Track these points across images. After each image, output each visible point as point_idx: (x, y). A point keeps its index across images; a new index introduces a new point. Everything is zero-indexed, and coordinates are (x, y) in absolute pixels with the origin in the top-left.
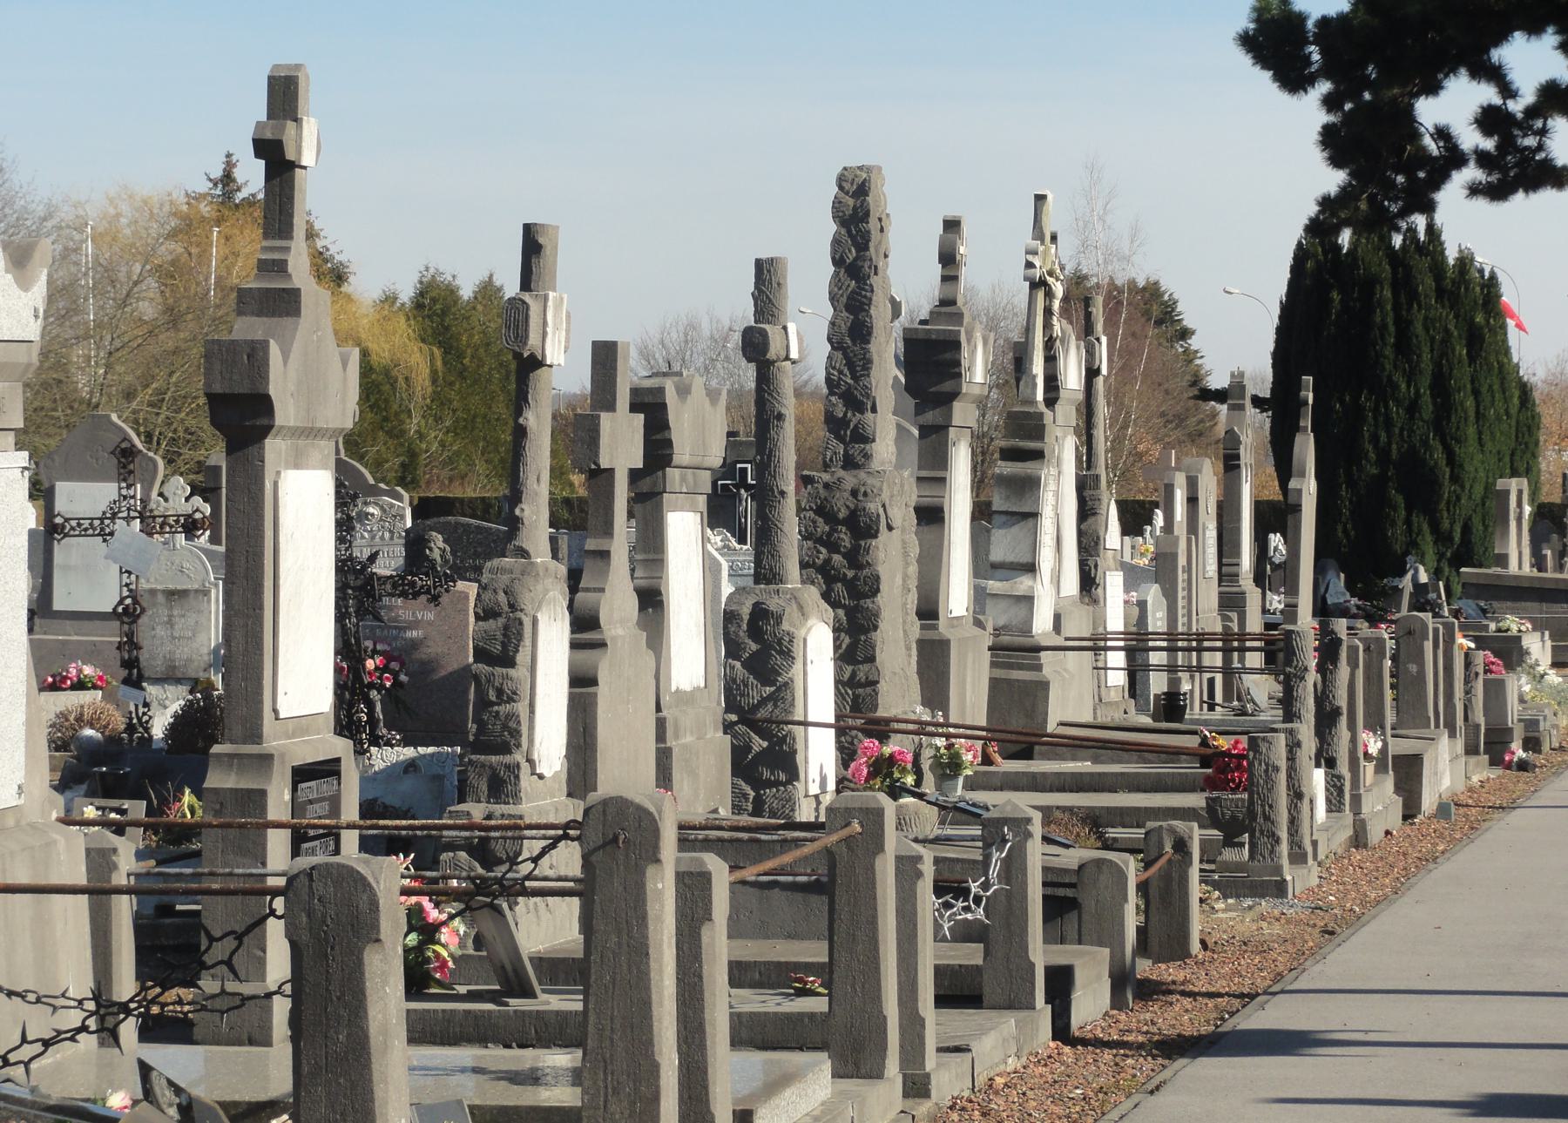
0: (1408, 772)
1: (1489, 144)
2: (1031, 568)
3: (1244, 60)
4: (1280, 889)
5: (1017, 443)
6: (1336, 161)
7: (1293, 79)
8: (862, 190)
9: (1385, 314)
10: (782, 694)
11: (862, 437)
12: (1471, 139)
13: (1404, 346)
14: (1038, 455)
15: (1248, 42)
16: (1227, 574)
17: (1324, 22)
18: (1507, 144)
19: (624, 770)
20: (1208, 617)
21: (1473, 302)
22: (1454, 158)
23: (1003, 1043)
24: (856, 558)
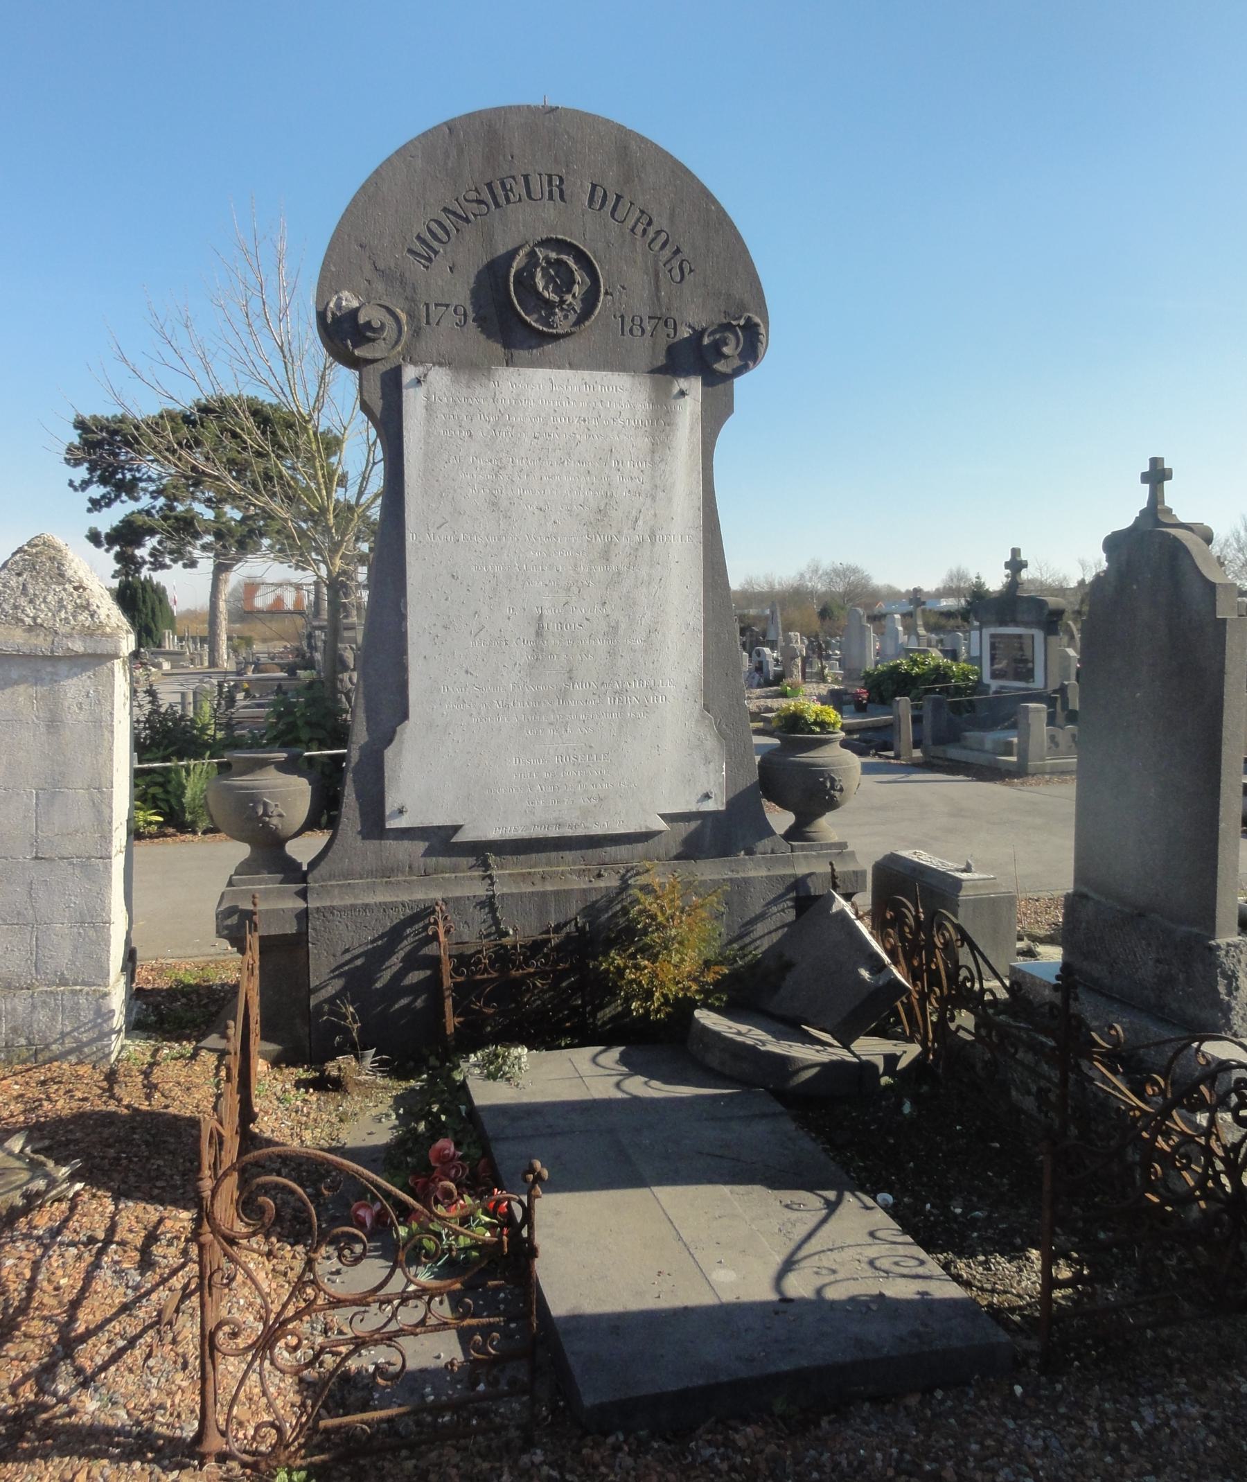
6: (118, 562)
9: (140, 595)
12: (148, 558)
13: (144, 602)
15: (87, 537)
18: (156, 560)
21: (158, 593)
22: (145, 562)
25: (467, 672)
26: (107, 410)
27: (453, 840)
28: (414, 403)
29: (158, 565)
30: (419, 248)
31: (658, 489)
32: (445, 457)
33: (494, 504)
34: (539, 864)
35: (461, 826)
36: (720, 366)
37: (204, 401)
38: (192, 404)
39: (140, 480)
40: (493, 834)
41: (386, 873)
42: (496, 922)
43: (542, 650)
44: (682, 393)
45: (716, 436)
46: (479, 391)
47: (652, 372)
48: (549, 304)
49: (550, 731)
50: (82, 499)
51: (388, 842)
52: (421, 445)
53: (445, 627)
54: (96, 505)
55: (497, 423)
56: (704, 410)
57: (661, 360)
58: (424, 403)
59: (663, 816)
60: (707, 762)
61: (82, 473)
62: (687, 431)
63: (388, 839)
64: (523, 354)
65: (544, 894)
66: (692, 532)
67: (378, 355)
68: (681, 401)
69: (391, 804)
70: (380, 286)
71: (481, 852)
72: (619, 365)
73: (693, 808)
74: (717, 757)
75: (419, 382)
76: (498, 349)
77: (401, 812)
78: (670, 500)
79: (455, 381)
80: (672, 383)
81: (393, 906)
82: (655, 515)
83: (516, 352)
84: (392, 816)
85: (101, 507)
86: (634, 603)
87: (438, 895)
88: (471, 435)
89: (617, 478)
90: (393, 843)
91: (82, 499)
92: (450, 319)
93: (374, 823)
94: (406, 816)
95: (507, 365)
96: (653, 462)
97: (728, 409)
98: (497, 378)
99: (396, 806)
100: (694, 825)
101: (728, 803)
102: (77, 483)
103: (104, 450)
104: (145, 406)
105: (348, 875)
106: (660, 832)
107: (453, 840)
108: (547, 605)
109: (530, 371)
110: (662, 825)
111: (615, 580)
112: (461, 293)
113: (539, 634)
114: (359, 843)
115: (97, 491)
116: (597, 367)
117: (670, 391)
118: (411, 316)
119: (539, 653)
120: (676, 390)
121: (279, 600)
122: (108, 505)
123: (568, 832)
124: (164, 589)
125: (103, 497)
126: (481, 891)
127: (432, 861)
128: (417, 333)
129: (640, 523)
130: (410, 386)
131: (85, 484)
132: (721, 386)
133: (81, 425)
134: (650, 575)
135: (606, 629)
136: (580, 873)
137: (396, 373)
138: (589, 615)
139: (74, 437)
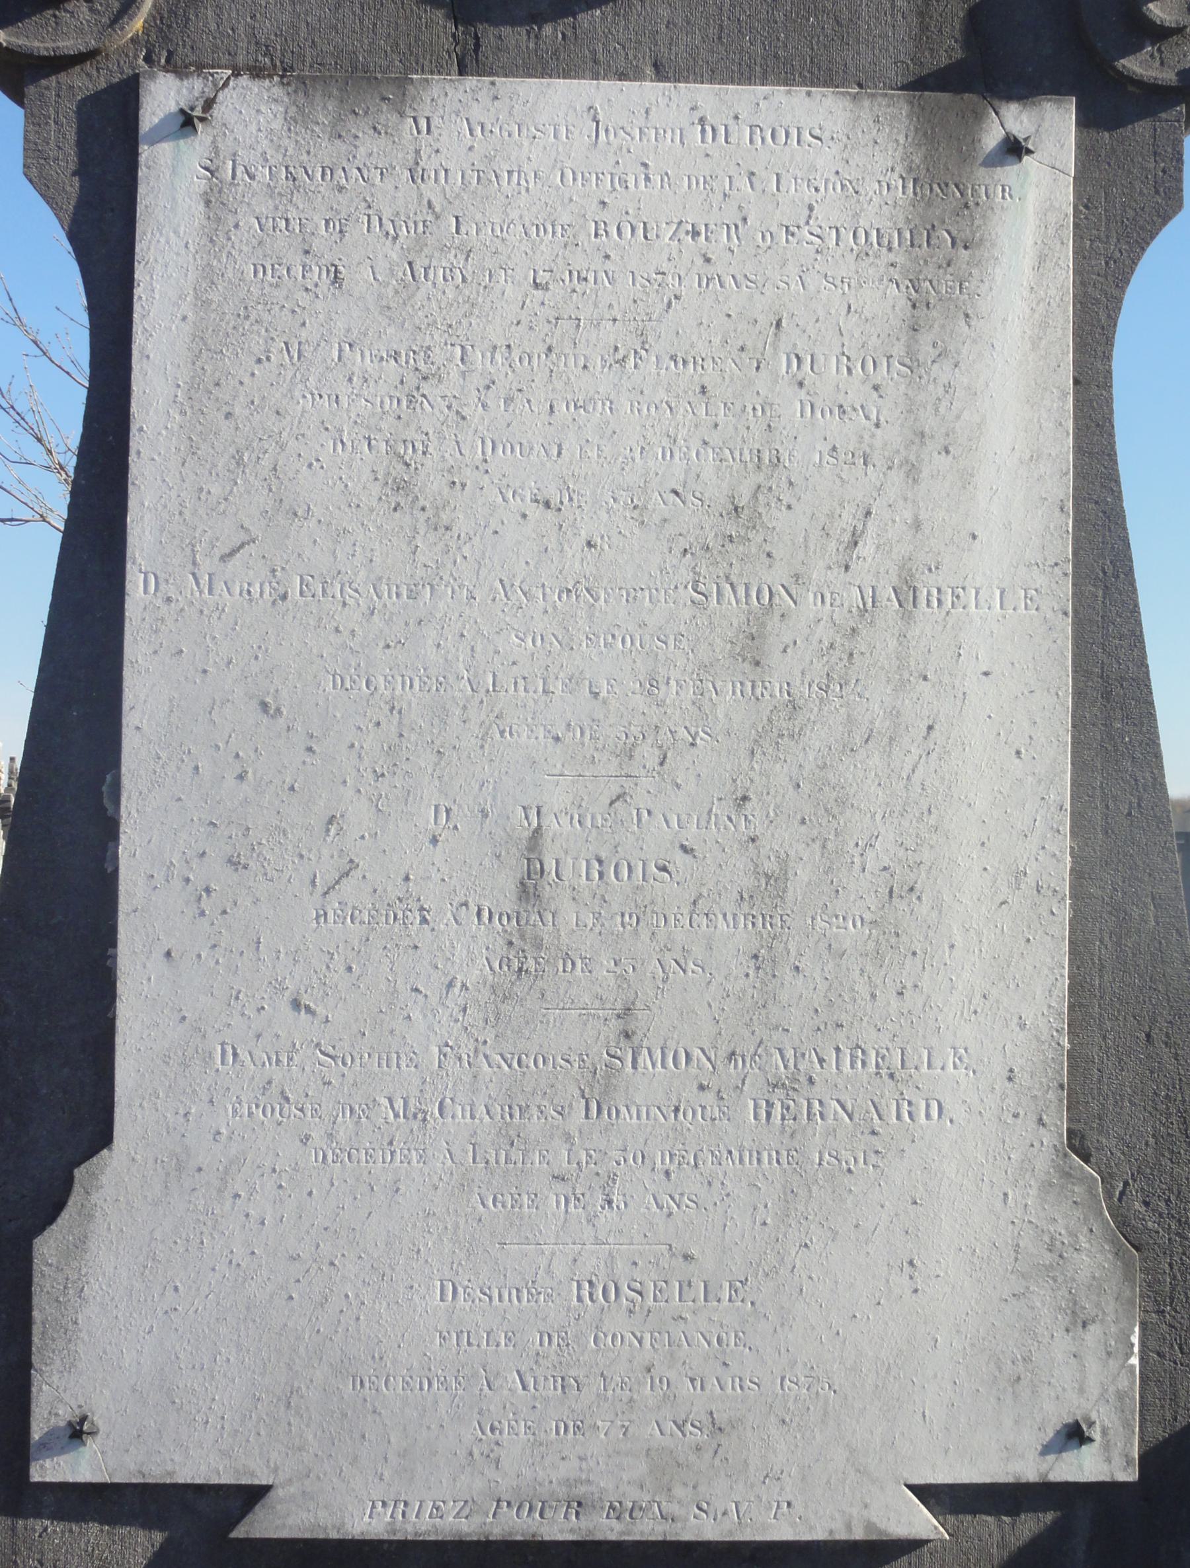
25: (296, 1004)
27: (239, 1533)
28: (170, 182)
31: (927, 445)
32: (257, 344)
33: (400, 487)
35: (266, 1489)
36: (1138, 65)
43: (538, 946)
44: (1014, 149)
45: (1122, 280)
46: (369, 146)
47: (918, 85)
49: (552, 1202)
51: (38, 1525)
52: (186, 308)
53: (233, 863)
55: (420, 244)
56: (1084, 202)
57: (948, 50)
58: (200, 185)
59: (925, 1493)
60: (1079, 1321)
62: (1027, 262)
63: (38, 1515)
64: (515, 37)
66: (1041, 581)
67: (69, 45)
68: (1010, 173)
72: (818, 73)
73: (1028, 1468)
74: (1110, 1307)
75: (187, 122)
76: (439, 27)
77: (77, 1432)
78: (966, 479)
79: (299, 119)
80: (979, 117)
82: (917, 525)
83: (489, 34)
84: (49, 1446)
86: (842, 803)
88: (337, 279)
89: (790, 406)
90: (56, 1528)
94: (92, 1446)
95: (462, 72)
96: (912, 362)
97: (1167, 201)
98: (426, 109)
99: (65, 1415)
100: (1029, 1526)
101: (1146, 1460)
106: (914, 1545)
107: (239, 1533)
108: (556, 798)
109: (528, 88)
110: (921, 1522)
111: (782, 725)
113: (528, 891)
116: (745, 76)
117: (975, 142)
119: (526, 953)
120: (992, 137)
129: (866, 549)
130: (159, 136)
132: (1142, 128)
134: (895, 714)
135: (747, 882)
137: (126, 97)
138: (691, 835)
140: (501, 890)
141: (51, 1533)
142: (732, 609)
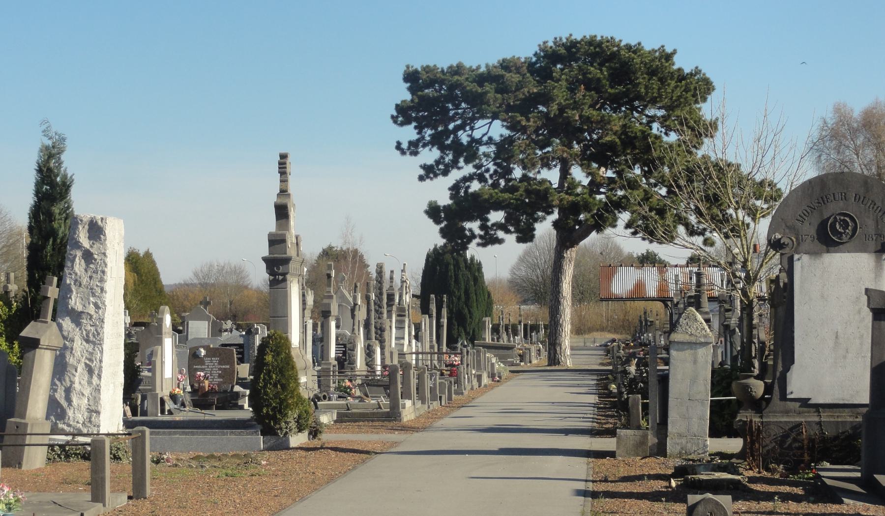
0: (479, 378)
1: (482, 233)
2: (403, 338)
3: (426, 217)
4: (462, 394)
5: (401, 313)
6: (443, 237)
7: (437, 221)
8: (381, 267)
9: (451, 273)
10: (373, 360)
11: (381, 313)
12: (477, 231)
13: (457, 281)
14: (404, 316)
15: (427, 212)
16: (431, 341)
17: (444, 207)
18: (487, 233)
19: (388, 362)
20: (428, 350)
21: (475, 268)
22: (473, 236)
23: (436, 405)
24: (381, 336)
26: (443, 60)
28: (797, 266)
29: (489, 240)
30: (799, 218)
34: (837, 412)
37: (551, 44)
38: (537, 49)
39: (479, 142)
40: (821, 401)
41: (787, 412)
42: (822, 430)
46: (818, 261)
47: (875, 252)
48: (841, 233)
50: (413, 165)
54: (429, 172)
57: (879, 248)
61: (409, 133)
64: (832, 249)
65: (838, 422)
69: (789, 390)
70: (787, 231)
71: (818, 407)
72: (865, 251)
76: (825, 247)
81: (789, 422)
85: (436, 175)
87: (803, 420)
91: (413, 165)
92: (809, 240)
93: (783, 397)
102: (405, 146)
103: (434, 104)
104: (481, 54)
105: (775, 412)
112: (813, 231)
113: (837, 337)
114: (779, 402)
115: (430, 155)
118: (797, 239)
121: (640, 286)
122: (445, 173)
123: (847, 402)
124: (479, 265)
125: (438, 162)
126: (817, 419)
127: (802, 409)
128: (798, 244)
131: (414, 148)
133: (411, 77)
136: (850, 416)
139: (404, 94)
140: (834, 337)
141: (788, 402)
142: (857, 307)
